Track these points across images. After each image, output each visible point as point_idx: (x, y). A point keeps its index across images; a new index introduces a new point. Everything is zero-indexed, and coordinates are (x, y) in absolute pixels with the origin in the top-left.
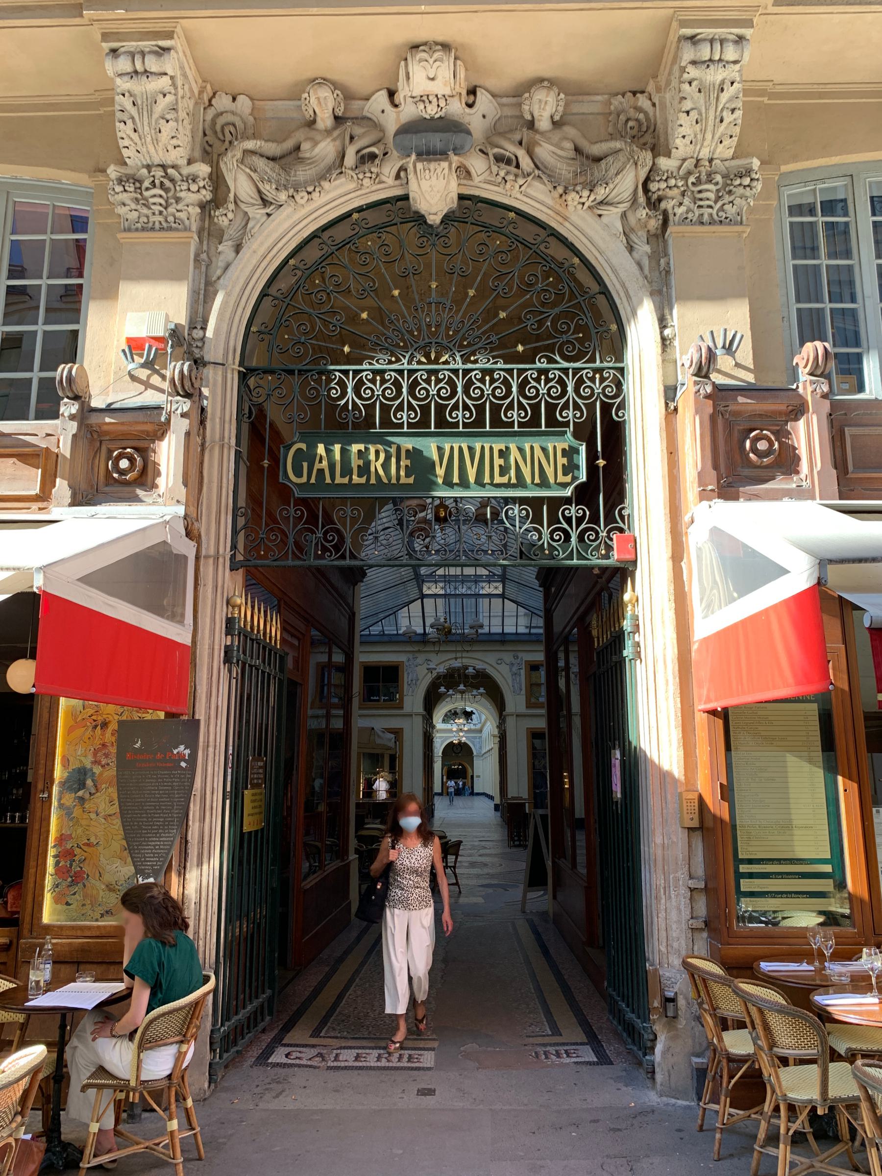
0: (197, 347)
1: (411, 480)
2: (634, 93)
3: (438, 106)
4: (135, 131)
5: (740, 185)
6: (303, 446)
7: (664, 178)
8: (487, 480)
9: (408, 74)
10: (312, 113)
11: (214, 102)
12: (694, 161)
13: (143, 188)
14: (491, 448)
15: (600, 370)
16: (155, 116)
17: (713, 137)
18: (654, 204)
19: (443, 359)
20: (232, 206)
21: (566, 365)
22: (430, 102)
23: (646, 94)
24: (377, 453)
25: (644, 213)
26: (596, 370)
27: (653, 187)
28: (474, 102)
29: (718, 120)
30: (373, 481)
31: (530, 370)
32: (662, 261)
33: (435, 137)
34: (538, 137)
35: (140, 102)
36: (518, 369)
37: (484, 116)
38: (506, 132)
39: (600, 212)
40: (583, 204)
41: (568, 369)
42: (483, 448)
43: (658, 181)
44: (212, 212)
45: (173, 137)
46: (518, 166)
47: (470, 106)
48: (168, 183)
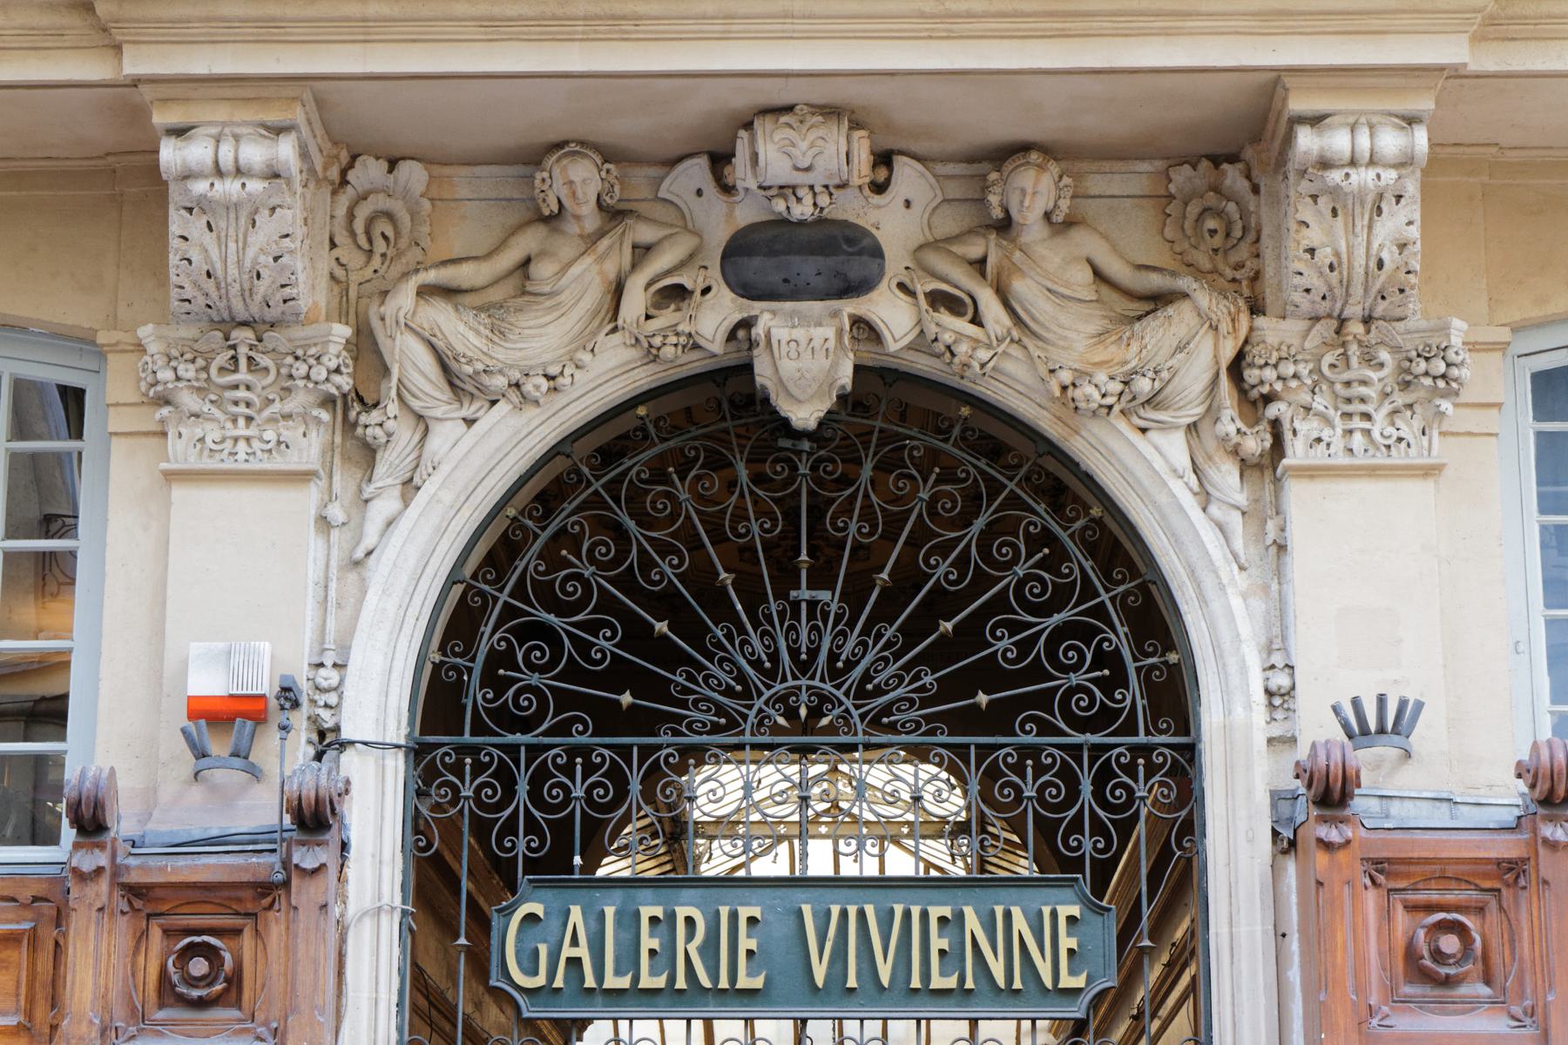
0: (326, 706)
1: (758, 983)
2: (1216, 160)
3: (815, 204)
4: (209, 275)
5: (1427, 374)
6: (537, 908)
7: (1273, 361)
8: (916, 983)
9: (755, 158)
10: (555, 209)
11: (351, 176)
12: (1334, 324)
13: (213, 371)
14: (925, 915)
15: (1146, 750)
16: (251, 252)
17: (1366, 290)
18: (1254, 403)
19: (825, 721)
20: (393, 408)
21: (1079, 738)
22: (799, 200)
23: (1240, 166)
24: (690, 921)
25: (1232, 429)
26: (1136, 750)
27: (1251, 375)
28: (888, 181)
29: (1373, 264)
30: (681, 983)
31: (1007, 745)
32: (1271, 526)
33: (807, 255)
34: (1018, 254)
35: (223, 224)
36: (978, 746)
37: (908, 204)
38: (950, 240)
39: (1143, 424)
40: (1110, 407)
41: (1079, 747)
42: (907, 915)
43: (1261, 367)
44: (352, 414)
45: (283, 286)
46: (976, 320)
47: (879, 188)
48: (264, 361)
